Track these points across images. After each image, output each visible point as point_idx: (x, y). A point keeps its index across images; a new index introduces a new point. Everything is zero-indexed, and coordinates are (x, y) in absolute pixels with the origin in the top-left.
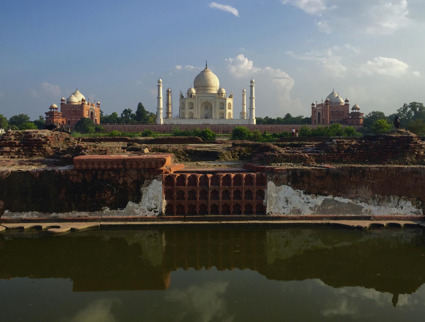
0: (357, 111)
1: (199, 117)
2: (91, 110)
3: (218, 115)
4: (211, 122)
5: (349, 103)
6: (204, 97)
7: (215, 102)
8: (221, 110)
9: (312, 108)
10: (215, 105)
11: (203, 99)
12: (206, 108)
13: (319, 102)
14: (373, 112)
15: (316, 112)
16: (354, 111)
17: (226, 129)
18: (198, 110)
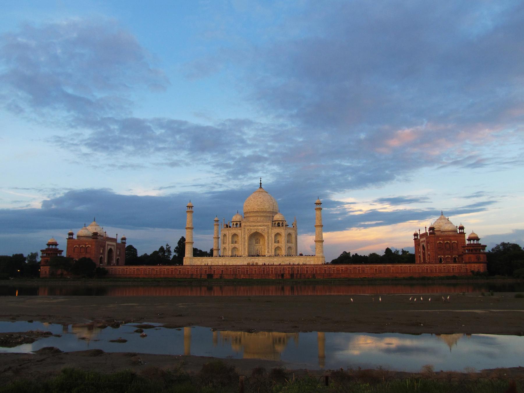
0: (475, 242)
1: (247, 254)
2: (109, 247)
3: (273, 251)
4: (260, 261)
5: (465, 231)
6: (254, 226)
7: (268, 233)
8: (277, 245)
9: (415, 239)
10: (268, 237)
11: (251, 229)
13: (423, 232)
14: (503, 244)
15: (419, 245)
16: (472, 242)
17: (280, 271)
18: (244, 245)
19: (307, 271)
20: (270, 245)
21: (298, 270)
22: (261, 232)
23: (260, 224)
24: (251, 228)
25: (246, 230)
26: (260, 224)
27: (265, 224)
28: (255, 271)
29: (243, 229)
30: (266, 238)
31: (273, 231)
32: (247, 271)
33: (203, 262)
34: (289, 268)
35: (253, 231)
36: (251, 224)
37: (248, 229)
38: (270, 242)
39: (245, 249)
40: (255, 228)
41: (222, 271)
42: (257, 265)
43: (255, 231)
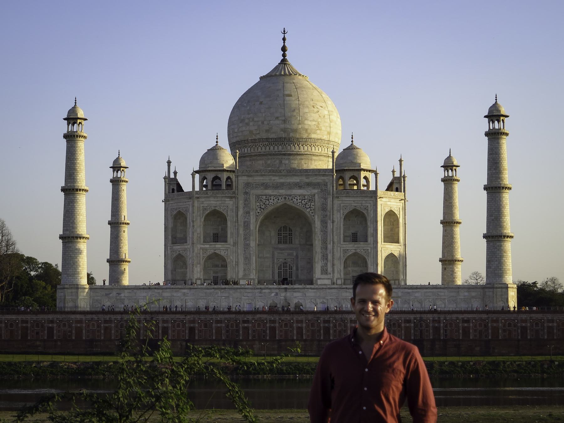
1: (253, 275)
3: (339, 266)
4: (309, 299)
6: (277, 186)
7: (324, 209)
8: (351, 247)
10: (324, 223)
12: (285, 236)
19: (466, 332)
20: (330, 246)
21: (437, 330)
22: (300, 207)
23: (296, 179)
24: (269, 192)
25: (253, 199)
26: (296, 179)
27: (313, 179)
28: (300, 329)
29: (241, 198)
30: (317, 225)
31: (336, 202)
32: (273, 329)
33: (122, 301)
34: (409, 321)
35: (274, 204)
36: (266, 179)
37: (258, 197)
38: (329, 238)
39: (247, 259)
40: (282, 192)
41: (192, 330)
42: (299, 311)
43: (281, 201)
